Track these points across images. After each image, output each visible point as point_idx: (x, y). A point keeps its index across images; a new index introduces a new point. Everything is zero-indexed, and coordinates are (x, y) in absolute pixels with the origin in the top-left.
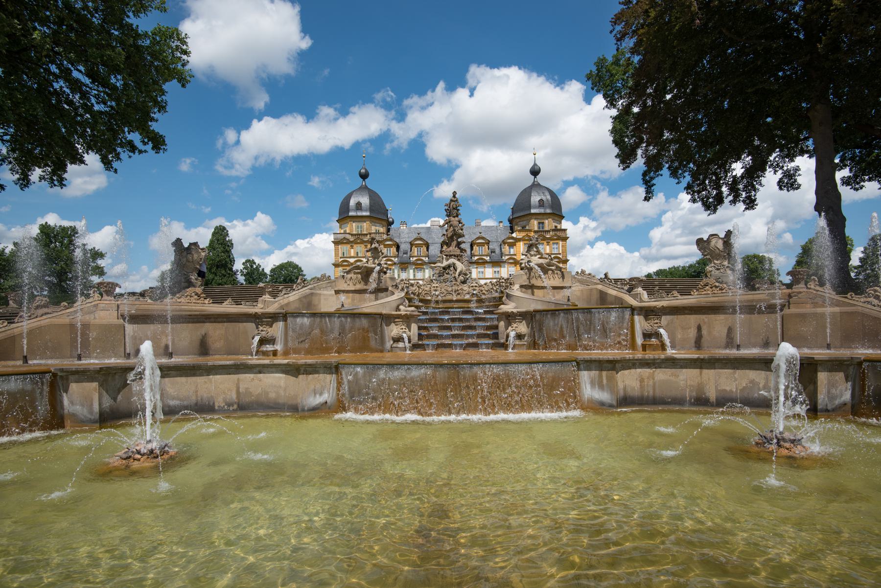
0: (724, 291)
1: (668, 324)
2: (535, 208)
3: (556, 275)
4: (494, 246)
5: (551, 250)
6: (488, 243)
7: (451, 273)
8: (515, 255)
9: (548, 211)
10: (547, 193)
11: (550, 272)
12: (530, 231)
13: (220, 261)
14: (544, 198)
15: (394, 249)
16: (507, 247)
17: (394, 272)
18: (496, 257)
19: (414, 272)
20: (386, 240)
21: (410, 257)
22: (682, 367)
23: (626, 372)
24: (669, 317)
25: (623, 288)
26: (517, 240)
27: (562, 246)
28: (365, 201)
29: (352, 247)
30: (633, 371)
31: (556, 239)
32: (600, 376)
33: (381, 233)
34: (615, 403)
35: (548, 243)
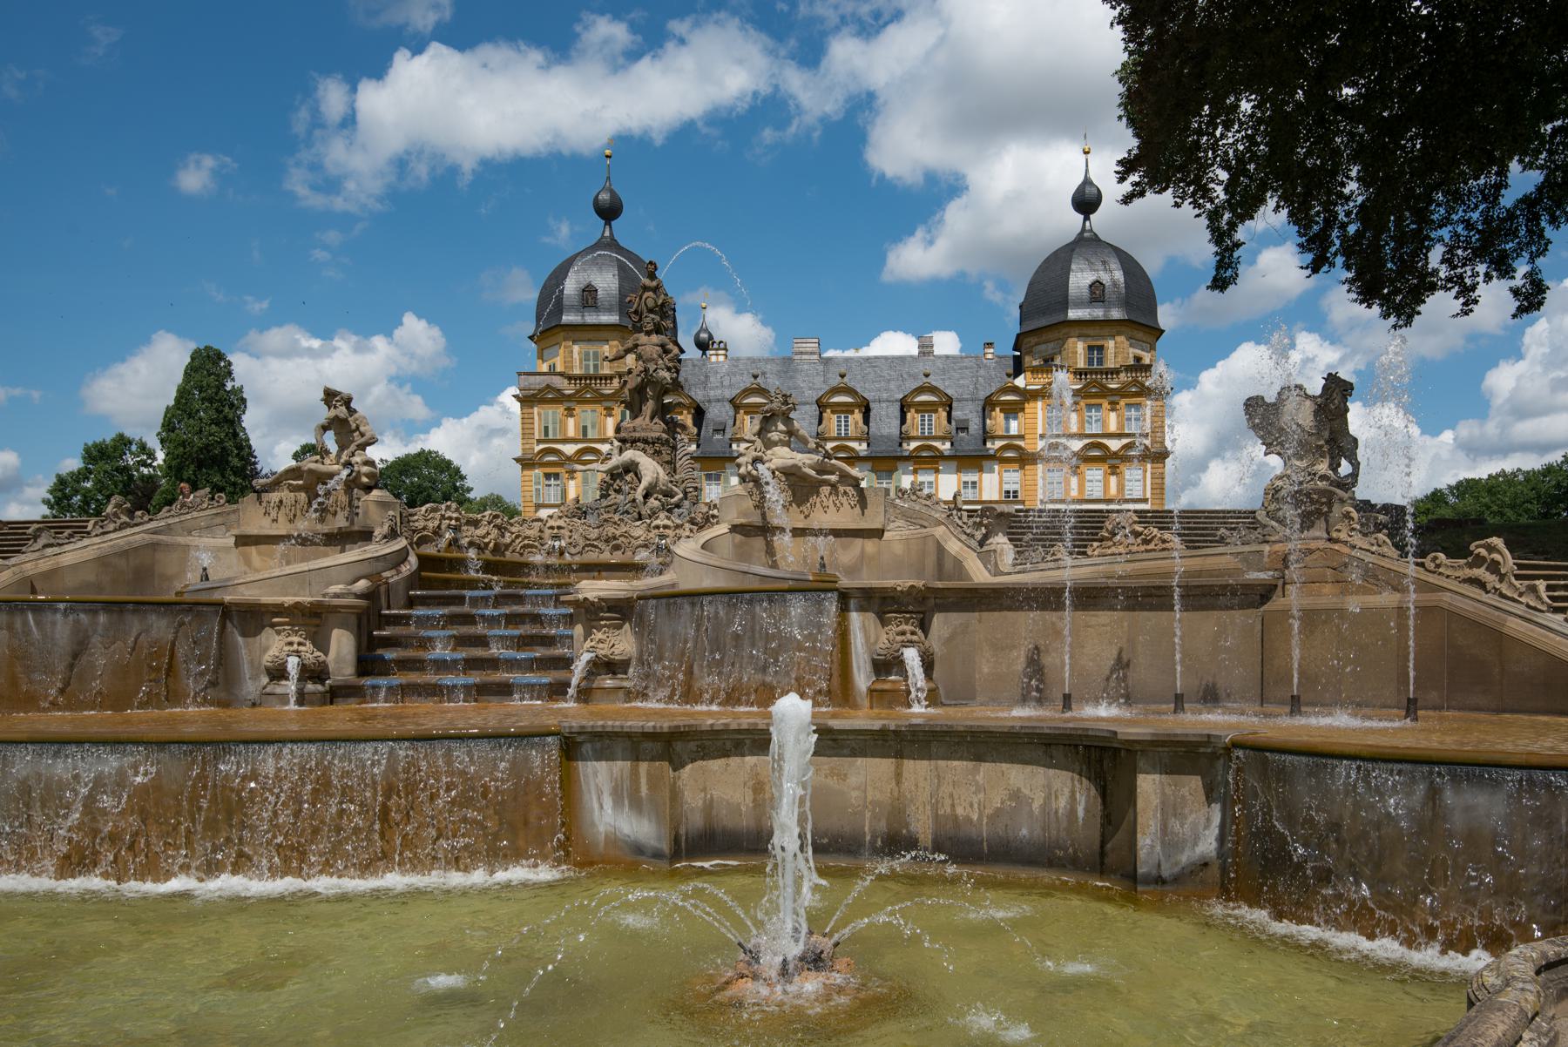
0: (1151, 546)
1: (951, 639)
2: (1080, 304)
3: (844, 500)
4: (967, 412)
5: (1120, 425)
6: (948, 405)
7: (626, 488)
8: (1021, 437)
9: (1116, 314)
10: (1114, 264)
11: (825, 490)
13: (207, 447)
14: (1105, 278)
16: (998, 415)
18: (968, 442)
22: (854, 753)
23: (715, 765)
24: (956, 618)
25: (973, 536)
26: (1029, 396)
29: (570, 412)
30: (734, 761)
32: (635, 775)
34: (665, 847)
35: (1114, 406)
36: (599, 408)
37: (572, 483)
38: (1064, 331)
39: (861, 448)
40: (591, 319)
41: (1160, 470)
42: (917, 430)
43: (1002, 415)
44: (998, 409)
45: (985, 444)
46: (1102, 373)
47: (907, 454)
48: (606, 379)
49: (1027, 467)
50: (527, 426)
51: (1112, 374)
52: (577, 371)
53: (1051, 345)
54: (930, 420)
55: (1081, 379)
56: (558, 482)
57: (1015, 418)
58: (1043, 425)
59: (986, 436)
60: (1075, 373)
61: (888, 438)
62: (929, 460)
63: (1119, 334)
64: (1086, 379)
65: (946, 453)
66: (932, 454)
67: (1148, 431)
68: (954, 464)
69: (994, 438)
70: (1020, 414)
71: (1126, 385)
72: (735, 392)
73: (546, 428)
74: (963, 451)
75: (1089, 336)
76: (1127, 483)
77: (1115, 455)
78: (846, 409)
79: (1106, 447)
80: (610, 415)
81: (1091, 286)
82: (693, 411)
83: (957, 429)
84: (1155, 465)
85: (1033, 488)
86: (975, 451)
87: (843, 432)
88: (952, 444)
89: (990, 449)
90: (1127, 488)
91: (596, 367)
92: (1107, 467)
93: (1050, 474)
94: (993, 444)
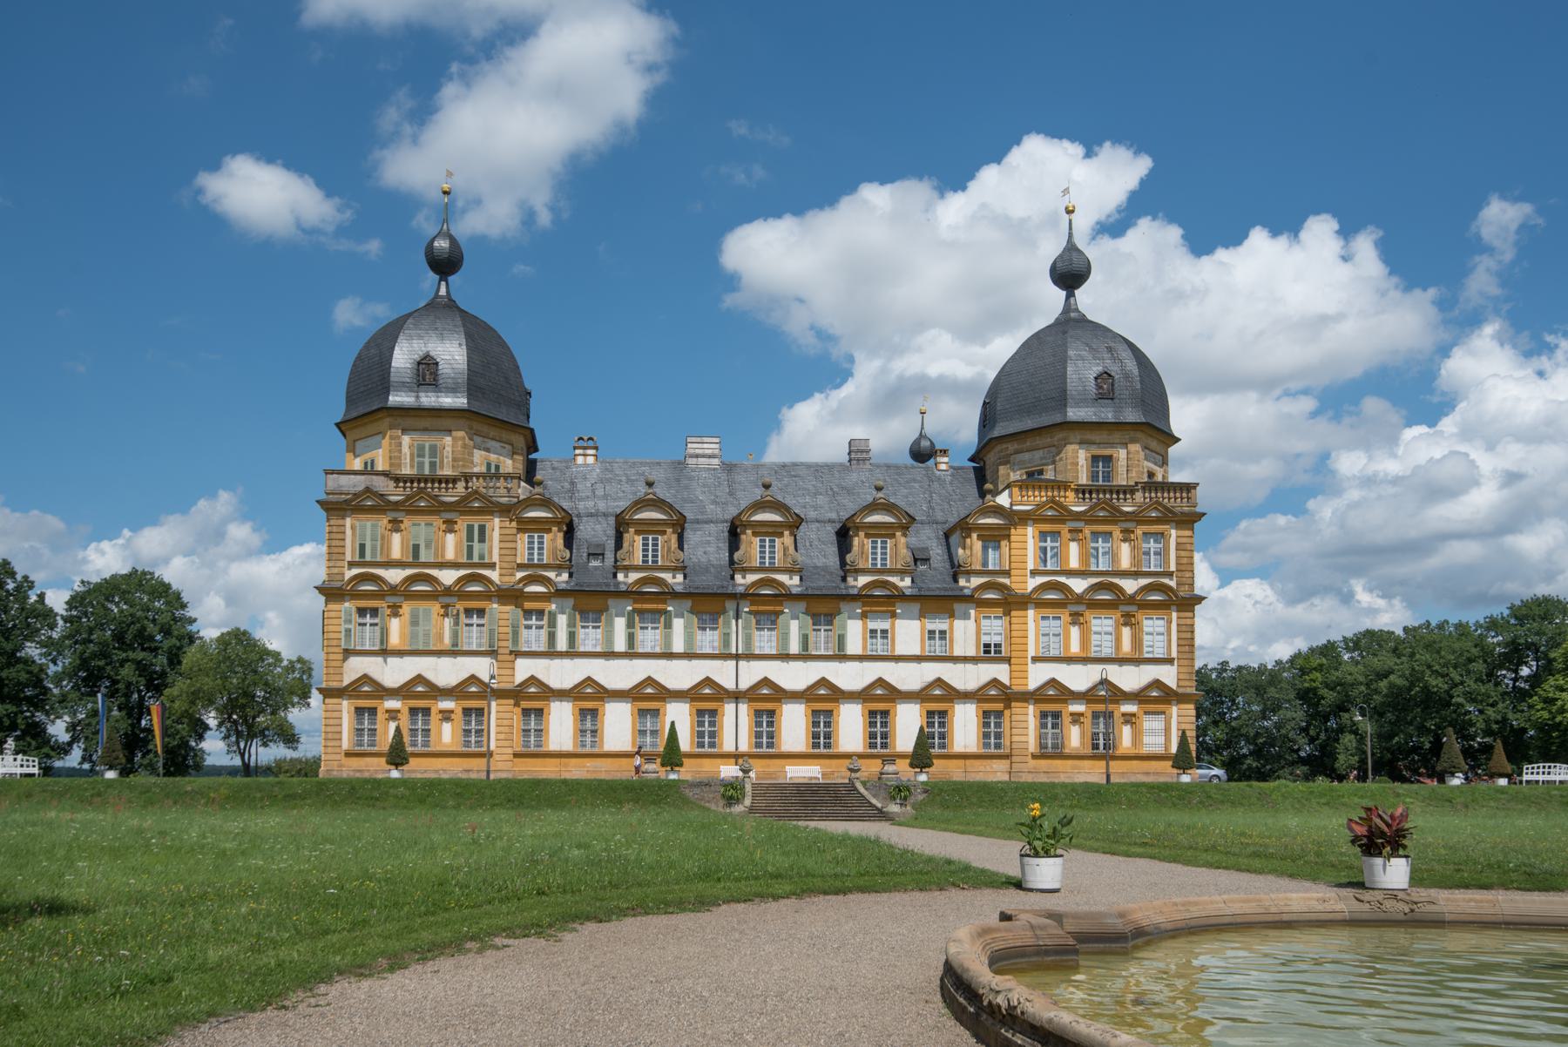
2: (1082, 402)
5: (1135, 559)
8: (1007, 573)
9: (1131, 415)
12: (1062, 486)
14: (1114, 369)
15: (553, 540)
17: (552, 623)
18: (935, 578)
19: (630, 625)
20: (530, 503)
21: (617, 568)
26: (1015, 519)
27: (1179, 547)
28: (452, 353)
29: (396, 525)
31: (1157, 521)
33: (507, 477)
35: (1127, 535)
36: (438, 522)
37: (395, 625)
38: (1059, 435)
39: (792, 582)
40: (428, 399)
41: (1189, 622)
42: (867, 560)
43: (980, 543)
44: (974, 536)
45: (956, 581)
46: (1111, 492)
47: (855, 592)
48: (447, 482)
49: (1013, 613)
50: (334, 543)
51: (1125, 493)
52: (407, 470)
53: (1038, 454)
54: (884, 548)
55: (1084, 499)
56: (376, 621)
57: (998, 547)
58: (1035, 558)
59: (957, 570)
60: (1077, 491)
61: (825, 568)
62: (882, 601)
63: (1133, 441)
64: (1091, 499)
65: (908, 592)
66: (889, 593)
67: (1173, 568)
68: (915, 607)
69: (969, 573)
70: (1004, 543)
71: (1143, 508)
72: (623, 504)
73: (362, 547)
74: (929, 589)
75: (1095, 444)
76: (1146, 637)
77: (1131, 600)
78: (773, 530)
79: (1119, 589)
80: (451, 531)
81: (1096, 378)
82: (565, 528)
83: (916, 560)
84: (1182, 614)
85: (1022, 641)
86: (945, 589)
87: (767, 560)
88: (913, 581)
89: (962, 588)
90: (1145, 643)
91: (433, 465)
92: (1119, 615)
93: (1046, 623)
94: (968, 581)
